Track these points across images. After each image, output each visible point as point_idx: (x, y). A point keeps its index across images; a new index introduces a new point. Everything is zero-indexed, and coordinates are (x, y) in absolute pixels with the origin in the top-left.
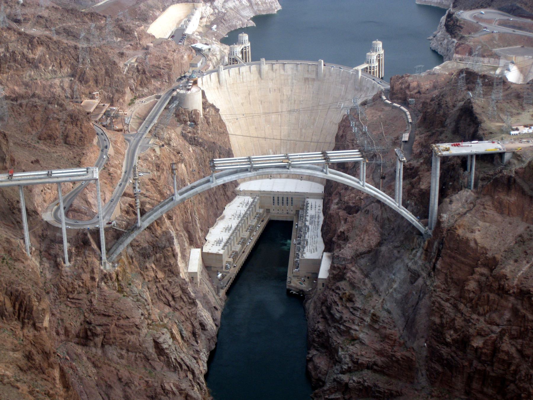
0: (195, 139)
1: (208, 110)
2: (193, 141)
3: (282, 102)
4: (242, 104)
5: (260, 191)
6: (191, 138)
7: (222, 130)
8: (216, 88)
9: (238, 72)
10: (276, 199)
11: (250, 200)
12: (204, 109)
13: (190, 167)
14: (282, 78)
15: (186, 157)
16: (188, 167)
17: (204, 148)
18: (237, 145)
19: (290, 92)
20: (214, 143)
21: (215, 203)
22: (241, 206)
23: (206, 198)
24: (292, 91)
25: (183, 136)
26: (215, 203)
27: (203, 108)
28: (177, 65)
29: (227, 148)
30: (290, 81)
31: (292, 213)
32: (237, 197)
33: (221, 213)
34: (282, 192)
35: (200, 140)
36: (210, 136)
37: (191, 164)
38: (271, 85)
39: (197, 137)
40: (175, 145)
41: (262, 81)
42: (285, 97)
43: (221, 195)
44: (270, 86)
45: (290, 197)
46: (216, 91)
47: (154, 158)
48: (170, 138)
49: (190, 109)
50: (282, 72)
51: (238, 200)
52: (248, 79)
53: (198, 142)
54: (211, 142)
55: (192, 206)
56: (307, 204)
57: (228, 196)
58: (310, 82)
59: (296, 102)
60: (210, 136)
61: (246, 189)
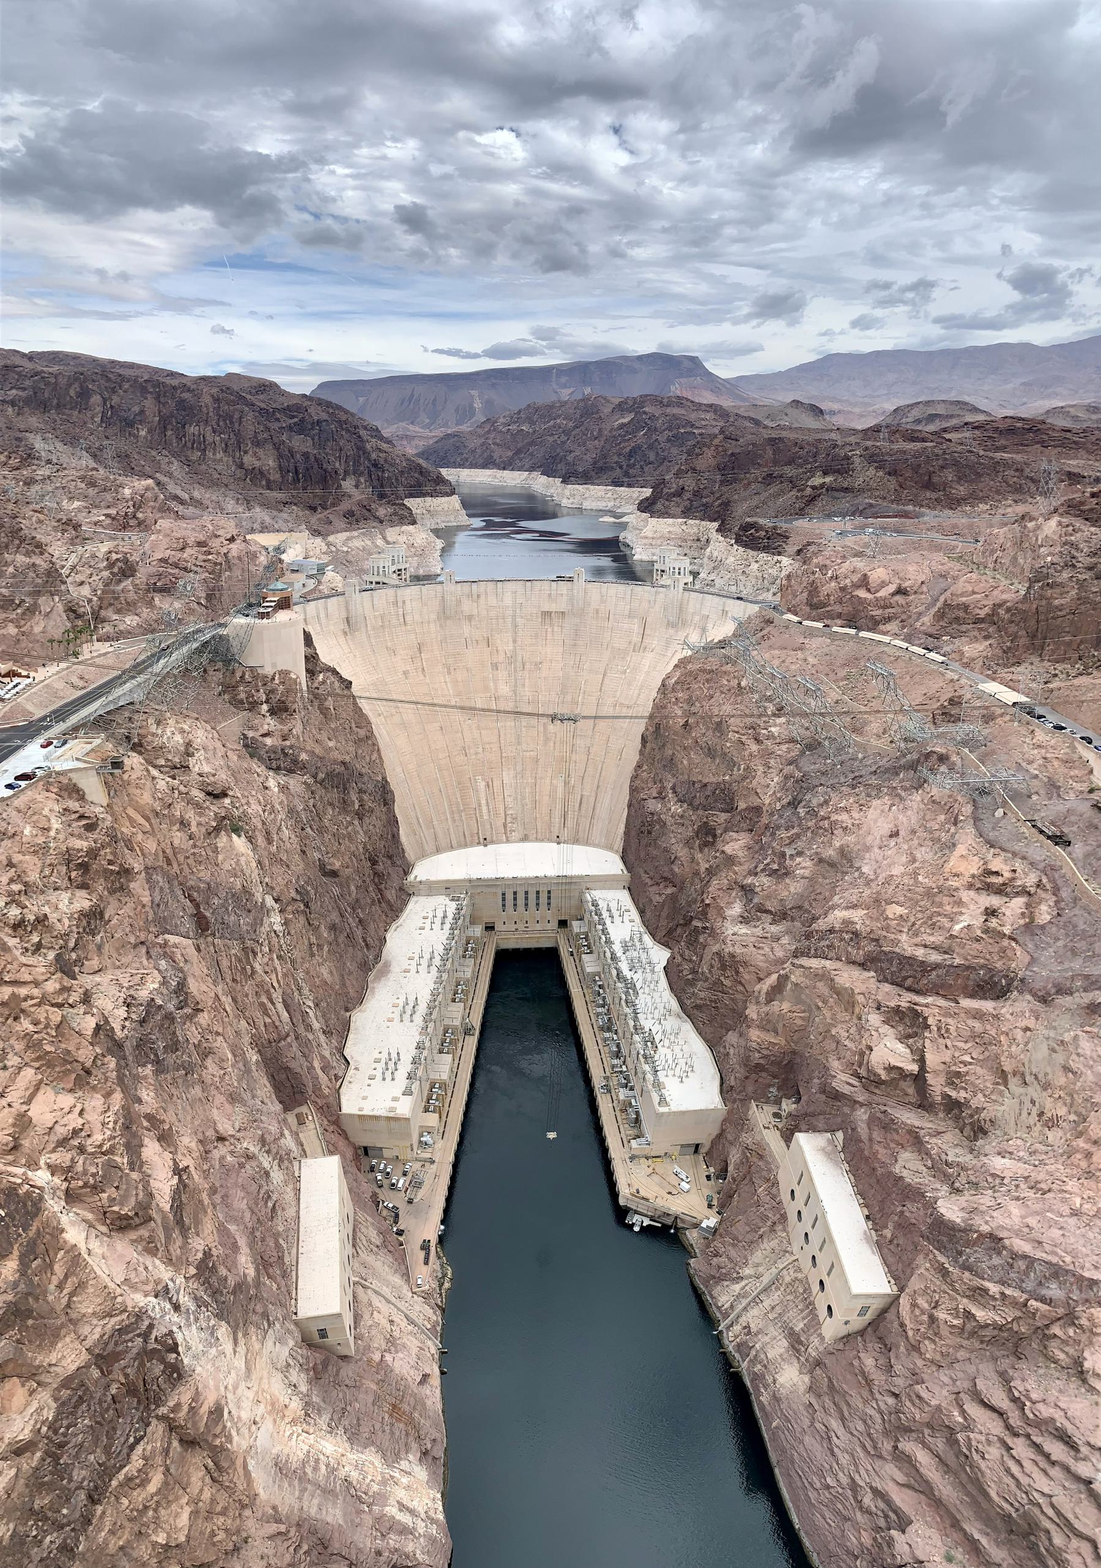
0: (286, 755)
1: (321, 677)
2: (283, 762)
3: (495, 666)
4: (405, 673)
5: (470, 881)
6: (273, 750)
7: (362, 733)
8: (340, 633)
9: (392, 599)
10: (509, 897)
11: (445, 905)
12: (311, 673)
13: (269, 841)
14: (493, 614)
15: (254, 808)
16: (261, 841)
17: (315, 777)
18: (399, 770)
19: (511, 644)
20: (343, 763)
21: (359, 933)
22: (428, 926)
23: (333, 927)
24: (515, 641)
25: (246, 746)
26: (359, 933)
27: (307, 671)
28: (237, 573)
29: (380, 778)
30: (509, 620)
31: (549, 926)
32: (413, 899)
33: (378, 957)
34: (525, 879)
35: (304, 756)
36: (331, 744)
37: (274, 831)
38: (466, 630)
39: (291, 747)
40: (207, 769)
41: (449, 622)
42: (501, 657)
43: (373, 902)
44: (466, 635)
45: (544, 890)
46: (342, 639)
47: (56, 824)
48: (189, 744)
49: (268, 670)
50: (493, 601)
51: (417, 909)
52: (417, 617)
53: (295, 761)
54: (335, 762)
55: (285, 975)
56: (595, 904)
57: (388, 902)
58: (555, 620)
59: (527, 666)
60: (331, 744)
61: (433, 879)
